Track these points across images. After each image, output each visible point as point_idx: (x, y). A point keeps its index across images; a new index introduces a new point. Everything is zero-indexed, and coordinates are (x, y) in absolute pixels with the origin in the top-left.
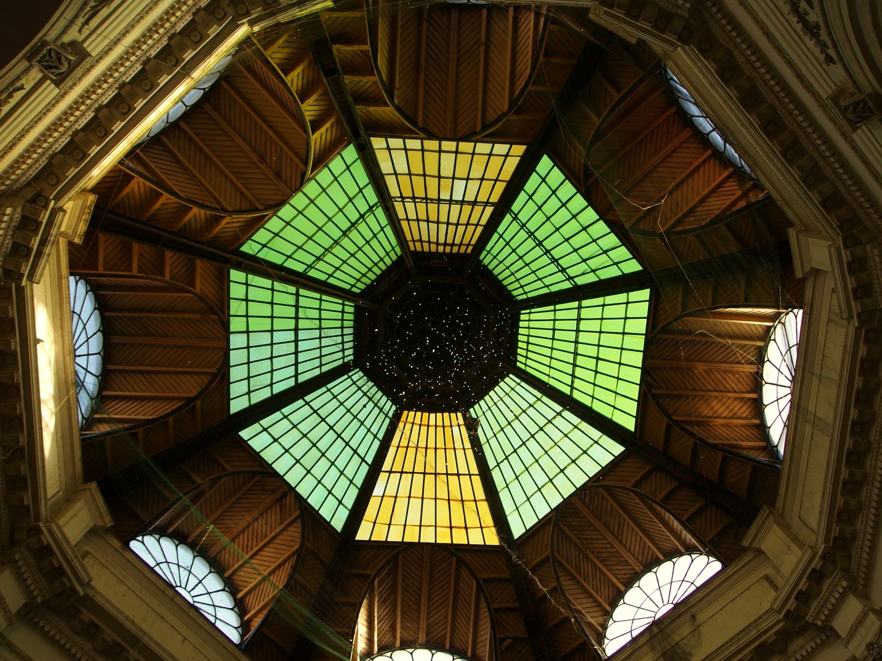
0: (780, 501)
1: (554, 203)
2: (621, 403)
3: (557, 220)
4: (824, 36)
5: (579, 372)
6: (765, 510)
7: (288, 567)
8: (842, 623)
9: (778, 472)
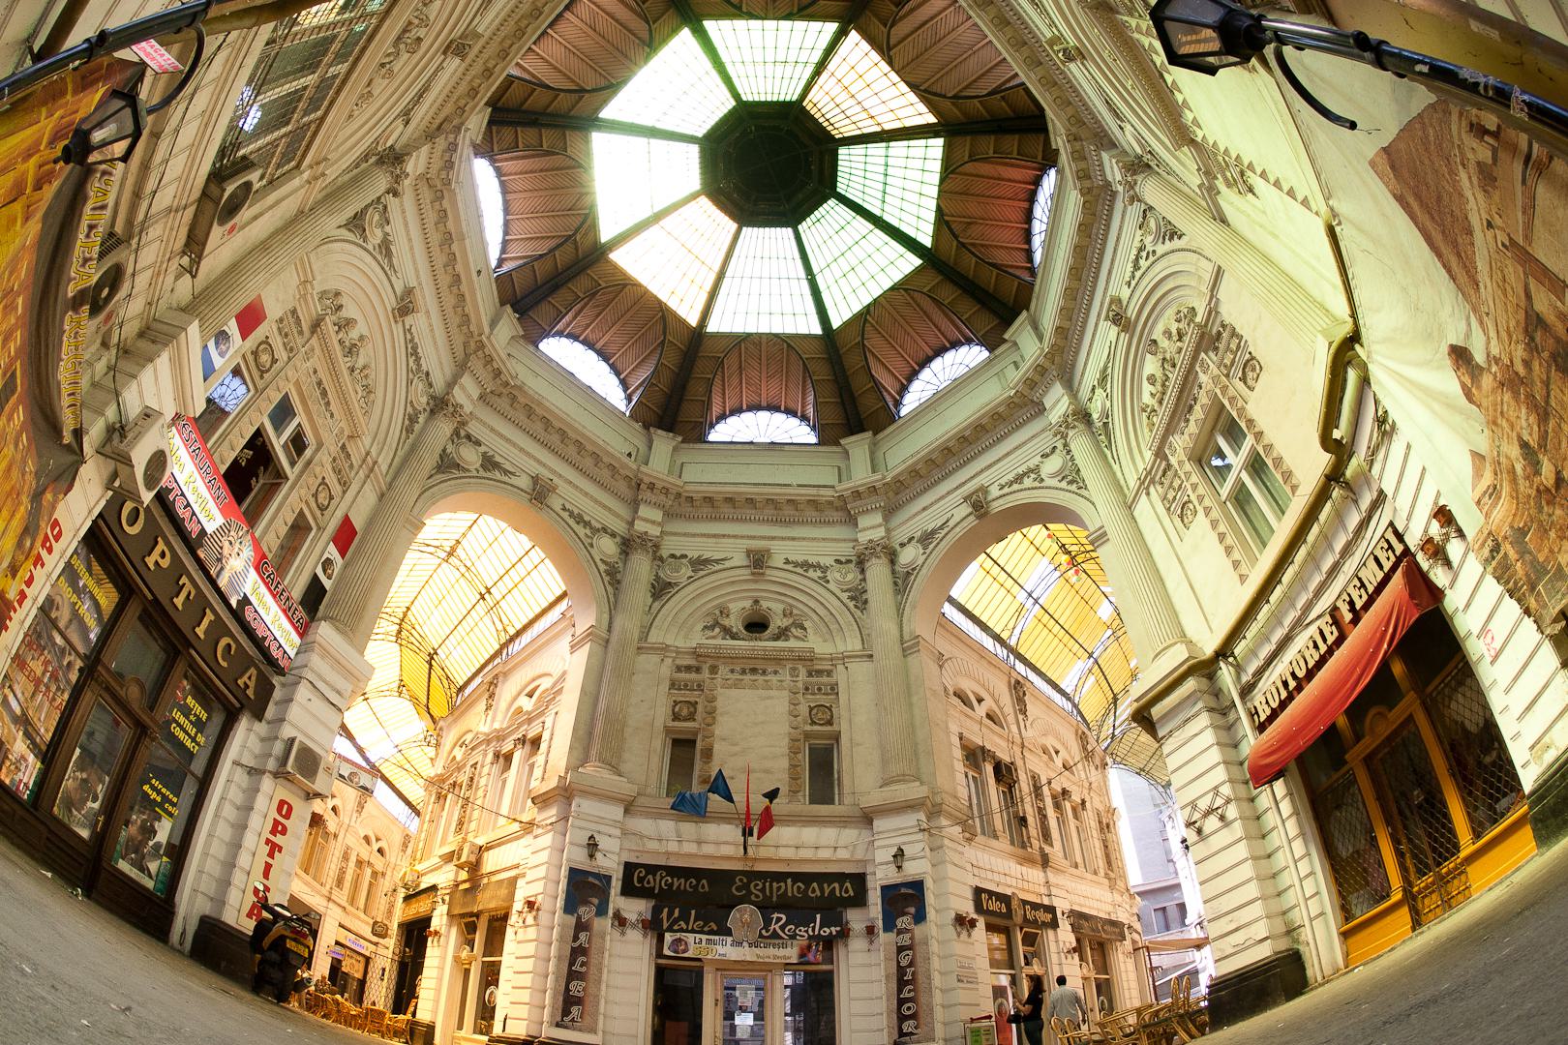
0: (881, 436)
1: (919, 164)
2: (842, 305)
3: (909, 174)
4: (1138, 274)
5: (834, 266)
6: (869, 434)
7: (553, 243)
8: (864, 521)
9: (894, 421)
